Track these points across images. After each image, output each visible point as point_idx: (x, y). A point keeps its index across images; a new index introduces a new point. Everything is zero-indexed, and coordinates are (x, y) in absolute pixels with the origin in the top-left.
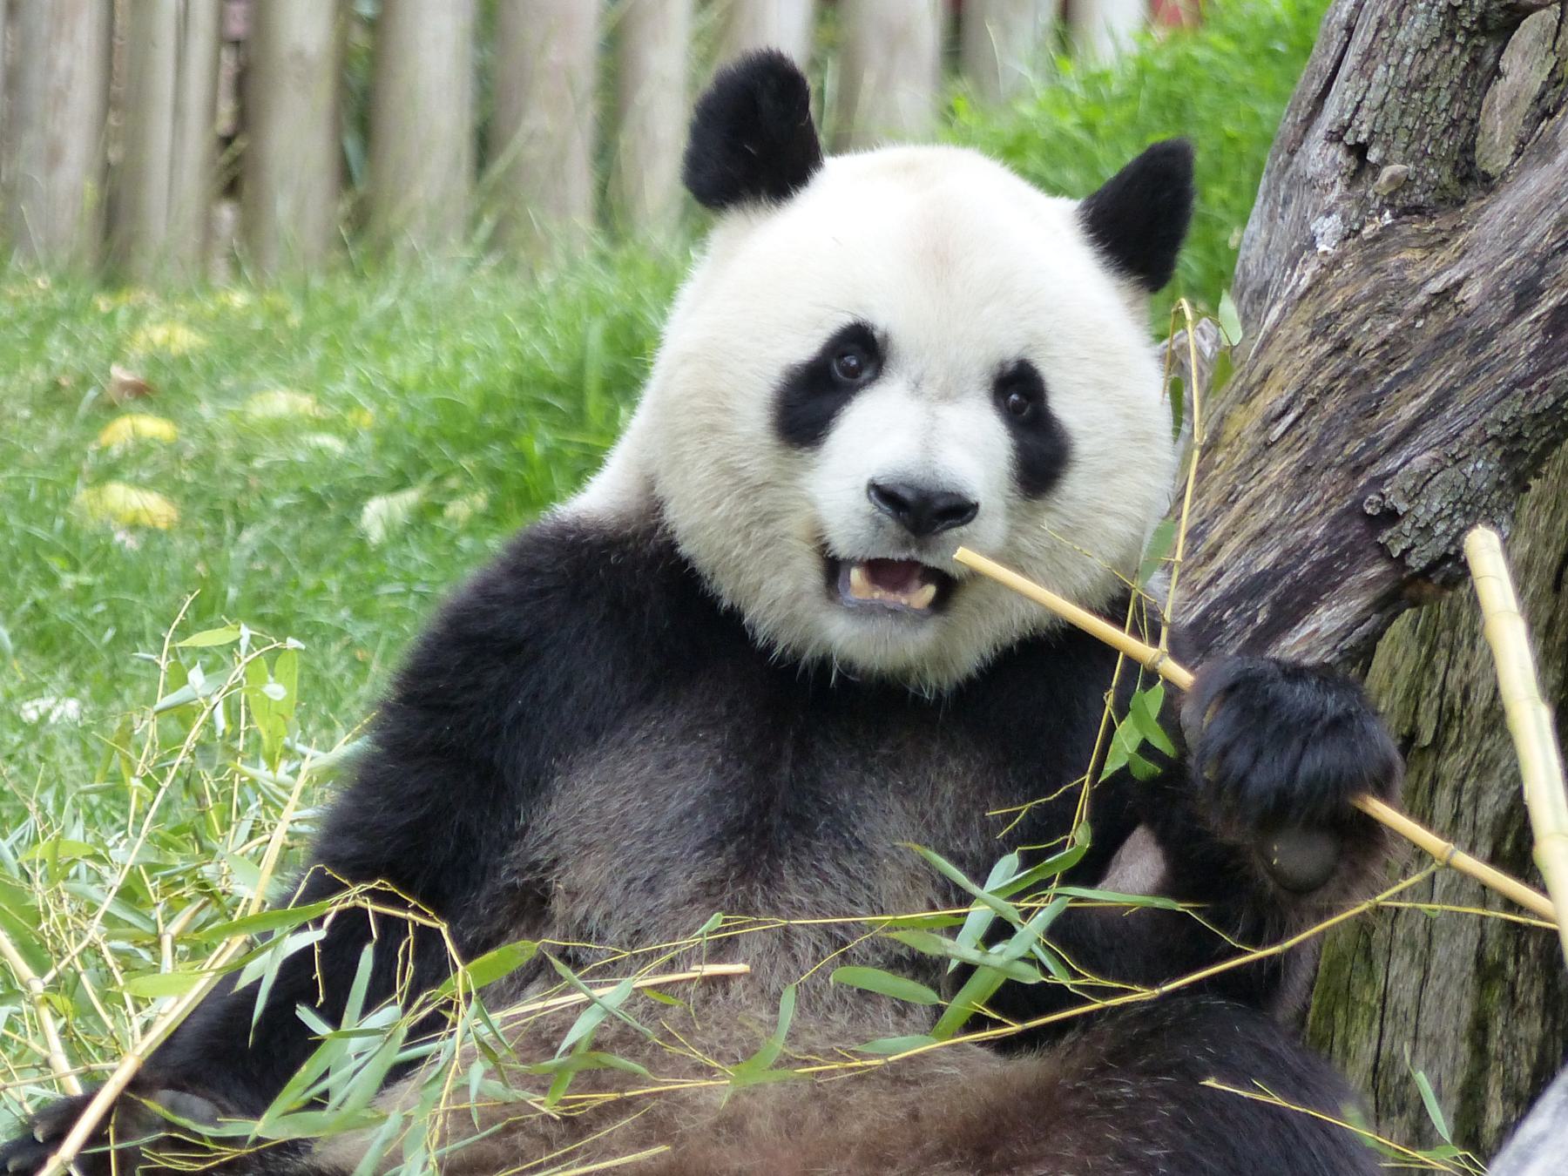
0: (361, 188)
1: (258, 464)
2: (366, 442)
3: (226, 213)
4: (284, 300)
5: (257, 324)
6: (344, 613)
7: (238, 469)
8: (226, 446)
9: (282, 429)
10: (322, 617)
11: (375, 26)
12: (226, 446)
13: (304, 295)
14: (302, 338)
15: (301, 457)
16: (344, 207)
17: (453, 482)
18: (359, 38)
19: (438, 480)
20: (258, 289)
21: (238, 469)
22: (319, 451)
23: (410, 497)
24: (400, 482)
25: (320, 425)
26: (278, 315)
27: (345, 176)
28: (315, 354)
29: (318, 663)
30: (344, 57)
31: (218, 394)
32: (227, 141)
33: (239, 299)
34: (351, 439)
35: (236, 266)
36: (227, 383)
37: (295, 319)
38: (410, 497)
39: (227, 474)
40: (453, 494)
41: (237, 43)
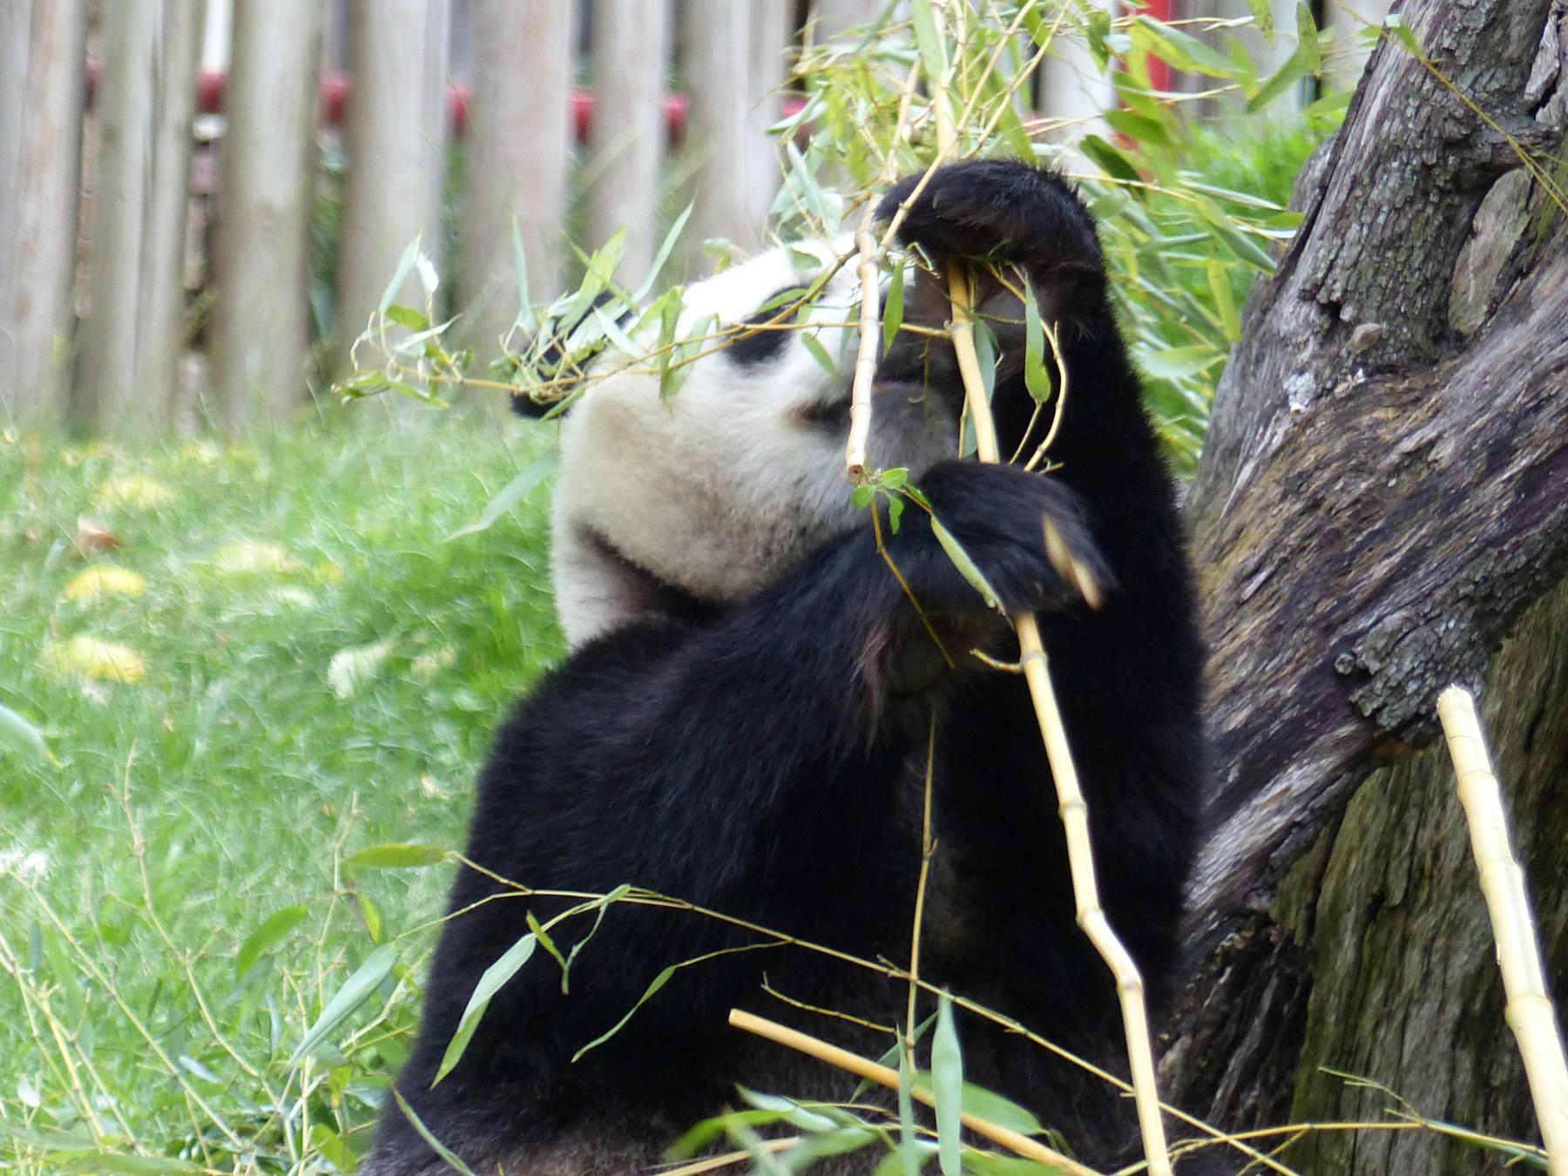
0: (327, 342)
1: (225, 618)
2: (334, 596)
3: (193, 367)
4: (251, 453)
5: (224, 478)
6: (311, 768)
7: (206, 623)
8: (194, 599)
9: (249, 584)
10: (289, 771)
11: (342, 180)
12: (194, 599)
13: (272, 449)
14: (271, 491)
15: (268, 611)
16: (307, 362)
17: (421, 637)
18: (327, 192)
19: (406, 635)
20: (225, 440)
21: (206, 623)
22: (286, 605)
23: (377, 652)
24: (368, 636)
25: (288, 578)
26: (245, 469)
27: (312, 330)
28: (283, 507)
29: (286, 819)
30: (311, 210)
31: (186, 547)
32: (194, 294)
33: (207, 452)
34: (319, 592)
35: (203, 425)
36: (194, 537)
37: (263, 473)
38: (377, 652)
39: (195, 628)
40: (420, 649)
41: (204, 197)
